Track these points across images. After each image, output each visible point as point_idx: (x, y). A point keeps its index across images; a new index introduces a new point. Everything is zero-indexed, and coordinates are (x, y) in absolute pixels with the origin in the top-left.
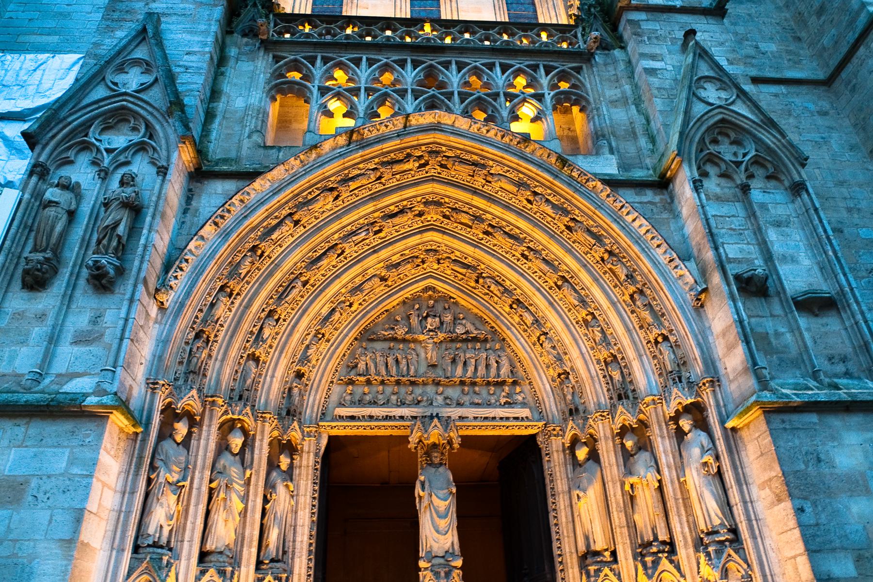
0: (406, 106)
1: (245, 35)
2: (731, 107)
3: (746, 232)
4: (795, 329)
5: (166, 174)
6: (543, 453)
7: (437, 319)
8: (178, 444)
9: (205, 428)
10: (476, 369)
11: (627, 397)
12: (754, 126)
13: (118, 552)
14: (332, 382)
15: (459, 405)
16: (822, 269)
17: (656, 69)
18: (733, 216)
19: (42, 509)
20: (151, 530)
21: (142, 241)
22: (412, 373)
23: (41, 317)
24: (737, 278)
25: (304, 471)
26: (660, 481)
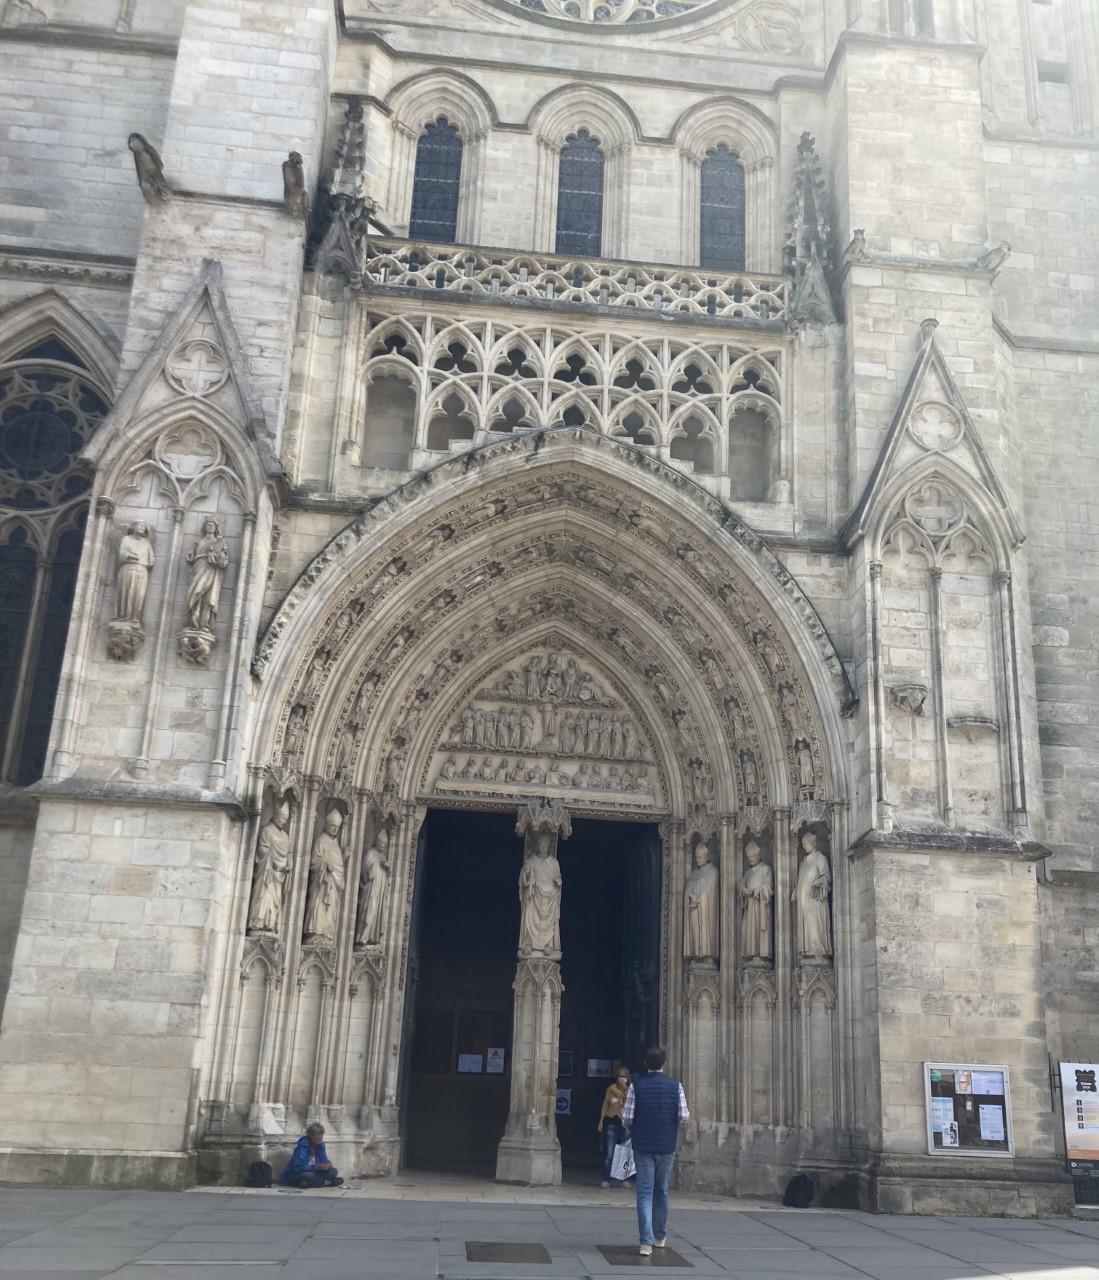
0: (540, 411)
1: (329, 272)
2: (947, 455)
3: (922, 633)
4: (941, 761)
5: (254, 523)
6: (665, 845)
7: (559, 680)
8: (280, 829)
9: (304, 811)
10: (599, 743)
11: (757, 804)
12: (973, 485)
13: (235, 935)
14: (433, 748)
15: (575, 785)
16: (997, 688)
17: (872, 378)
18: (913, 611)
19: (172, 897)
20: (261, 915)
21: (238, 614)
22: (524, 745)
23: (135, 694)
24: (892, 692)
25: (401, 849)
26: (773, 898)
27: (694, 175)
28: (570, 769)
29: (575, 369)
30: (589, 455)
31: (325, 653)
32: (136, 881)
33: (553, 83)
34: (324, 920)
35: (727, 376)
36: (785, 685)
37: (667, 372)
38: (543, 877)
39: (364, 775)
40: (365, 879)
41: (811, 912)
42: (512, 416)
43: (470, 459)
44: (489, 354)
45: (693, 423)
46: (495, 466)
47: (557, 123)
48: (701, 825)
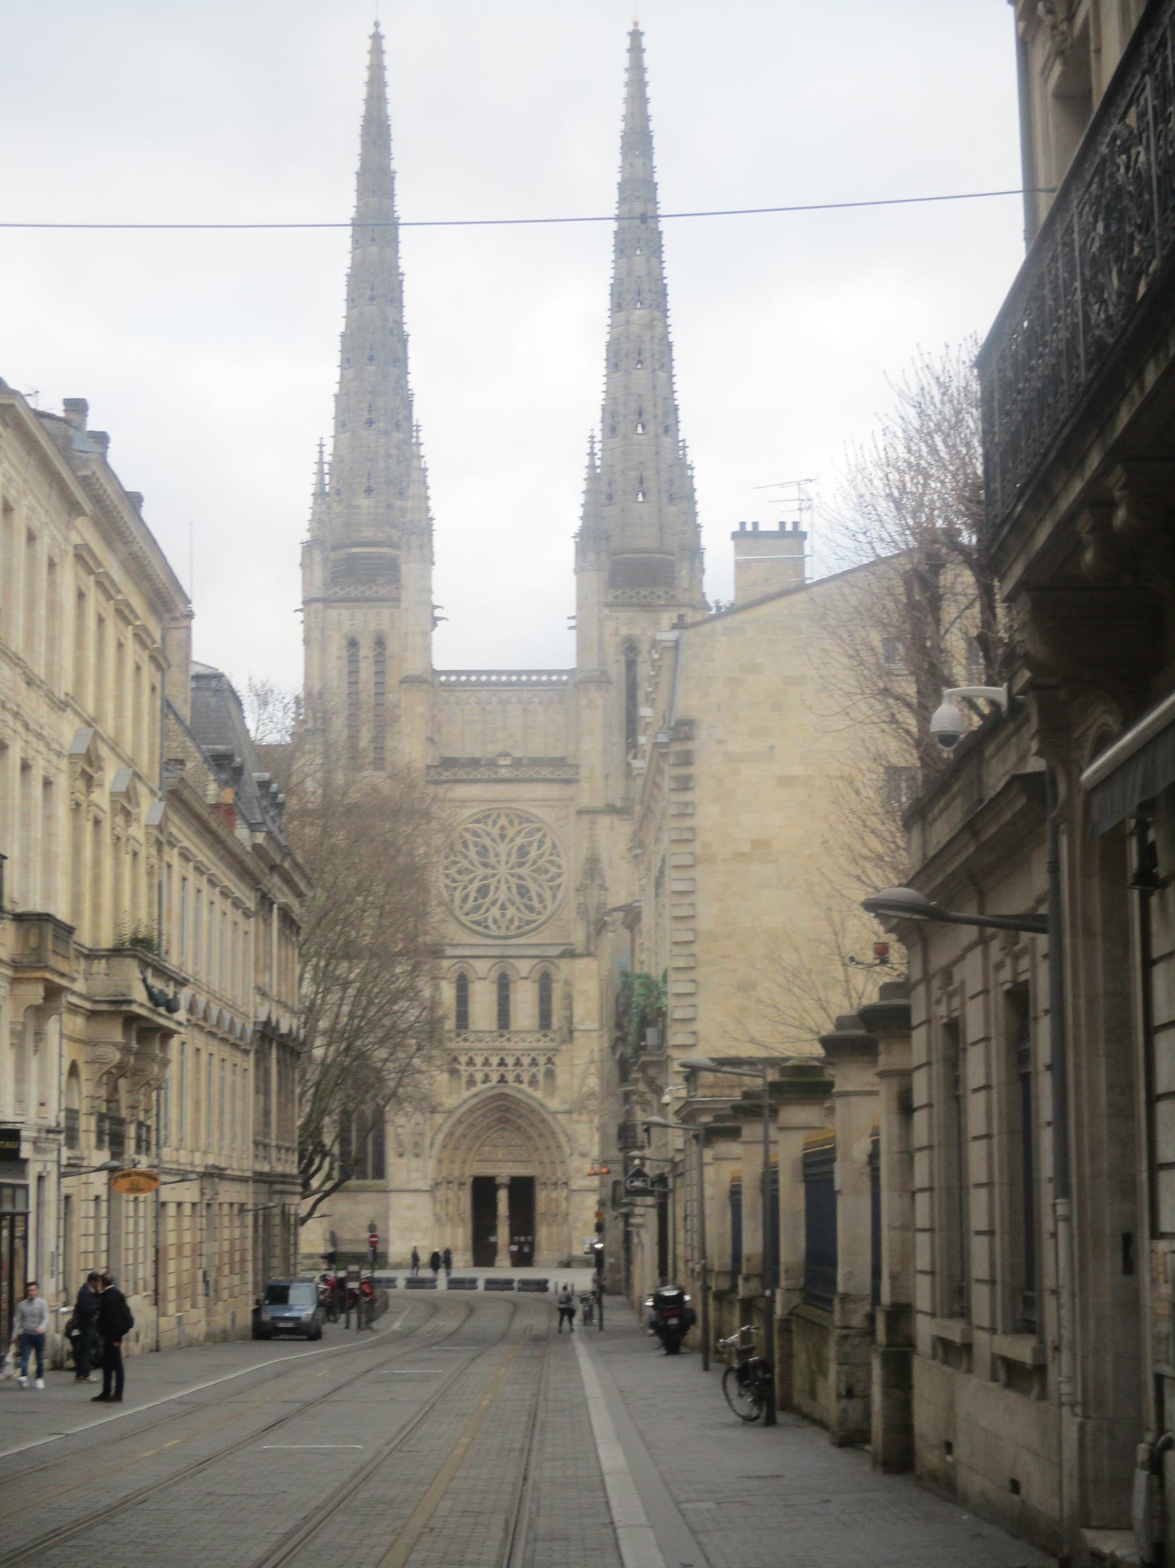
27: (536, 986)
28: (510, 1164)
29: (502, 1063)
30: (507, 1091)
31: (444, 1147)
32: (411, 1208)
33: (493, 961)
34: (450, 1210)
35: (542, 1060)
36: (559, 1147)
37: (526, 1061)
38: (503, 1196)
39: (456, 1174)
40: (459, 1199)
41: (564, 1204)
42: (486, 1079)
43: (475, 1095)
44: (479, 1060)
45: (534, 1076)
46: (483, 1096)
47: (494, 975)
48: (542, 1180)
